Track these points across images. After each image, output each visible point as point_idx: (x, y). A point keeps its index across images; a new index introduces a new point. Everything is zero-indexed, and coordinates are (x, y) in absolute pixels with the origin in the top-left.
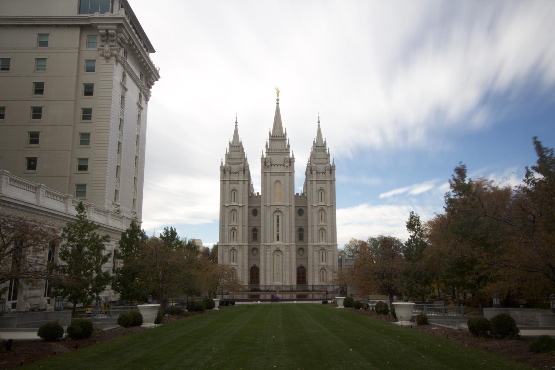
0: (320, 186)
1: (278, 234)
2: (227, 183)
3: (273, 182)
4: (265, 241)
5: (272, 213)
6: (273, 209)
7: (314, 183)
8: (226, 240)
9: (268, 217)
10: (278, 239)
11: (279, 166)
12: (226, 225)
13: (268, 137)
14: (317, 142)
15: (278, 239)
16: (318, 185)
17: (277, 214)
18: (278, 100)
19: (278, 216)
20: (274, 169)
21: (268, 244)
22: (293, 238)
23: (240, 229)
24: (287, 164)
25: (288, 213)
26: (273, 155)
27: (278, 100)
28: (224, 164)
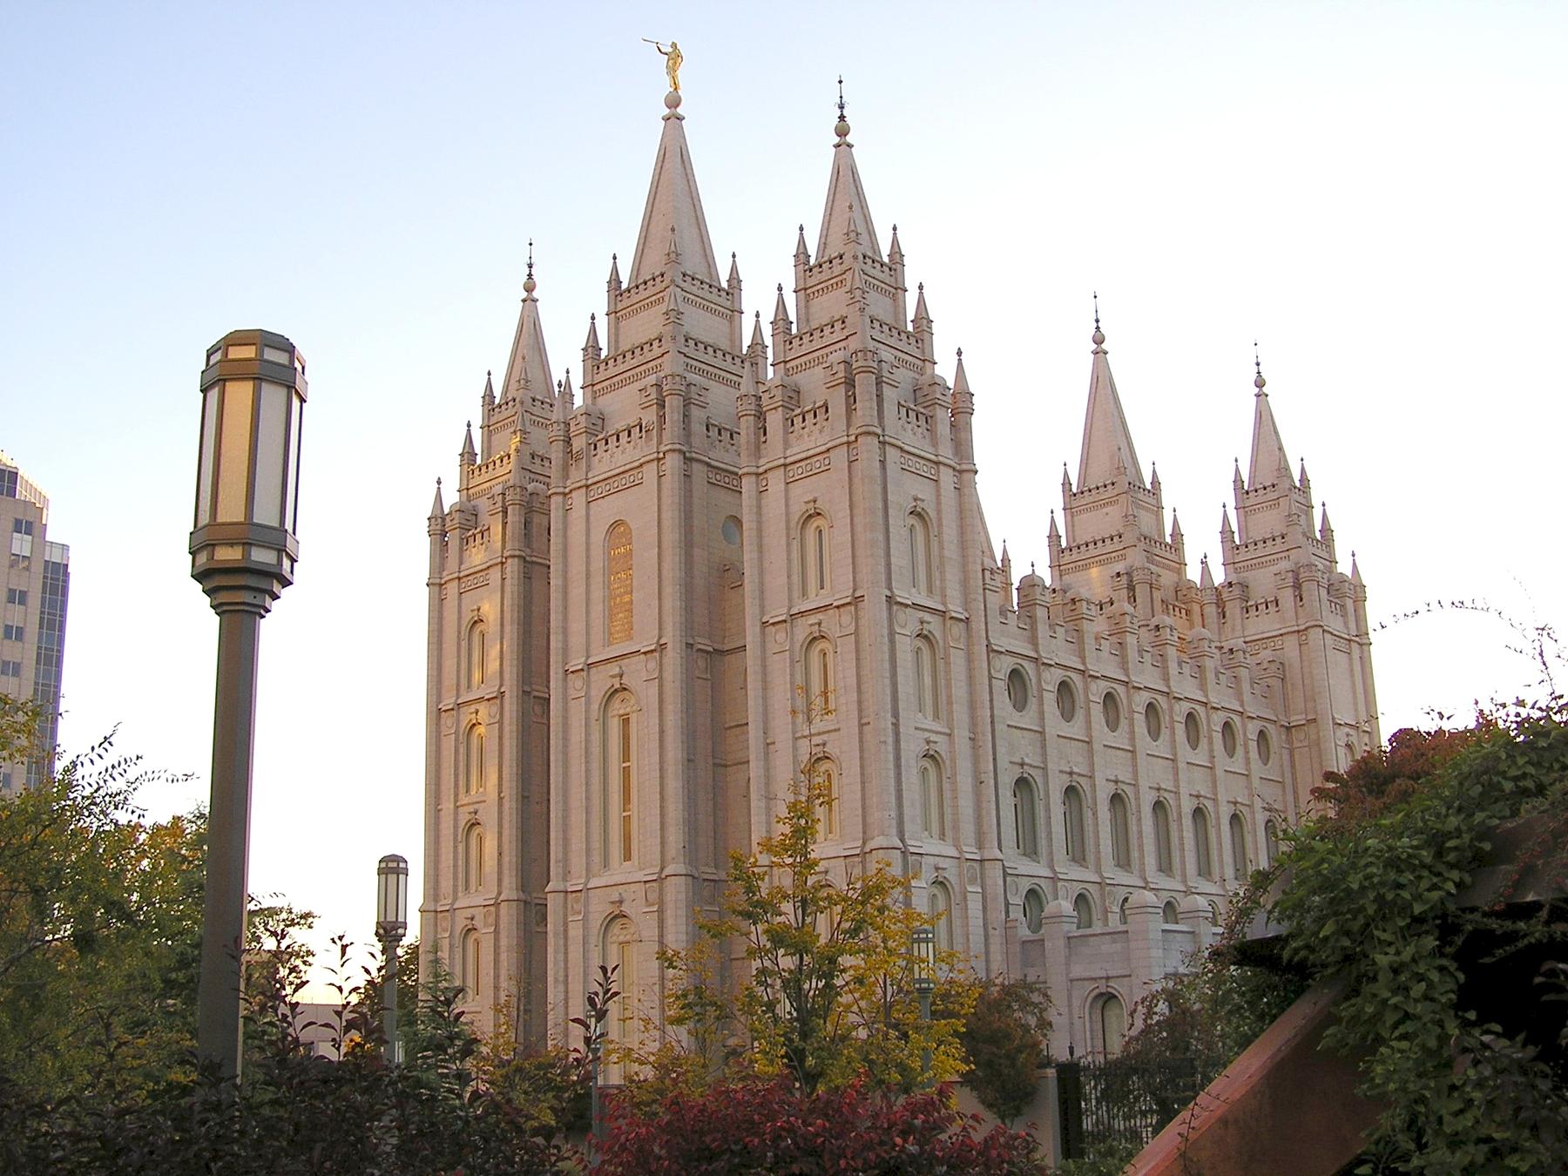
0: (802, 493)
1: (627, 820)
2: (452, 589)
3: (598, 535)
4: (566, 875)
5: (595, 706)
6: (602, 681)
7: (776, 481)
8: (446, 885)
9: (577, 735)
10: (627, 856)
11: (624, 437)
12: (447, 806)
13: (601, 305)
14: (823, 245)
15: (627, 856)
16: (797, 490)
17: (617, 707)
18: (673, 102)
19: (626, 721)
20: (607, 462)
21: (575, 883)
22: (675, 838)
23: (489, 816)
24: (650, 417)
25: (654, 689)
26: (613, 388)
27: (673, 102)
28: (451, 498)
